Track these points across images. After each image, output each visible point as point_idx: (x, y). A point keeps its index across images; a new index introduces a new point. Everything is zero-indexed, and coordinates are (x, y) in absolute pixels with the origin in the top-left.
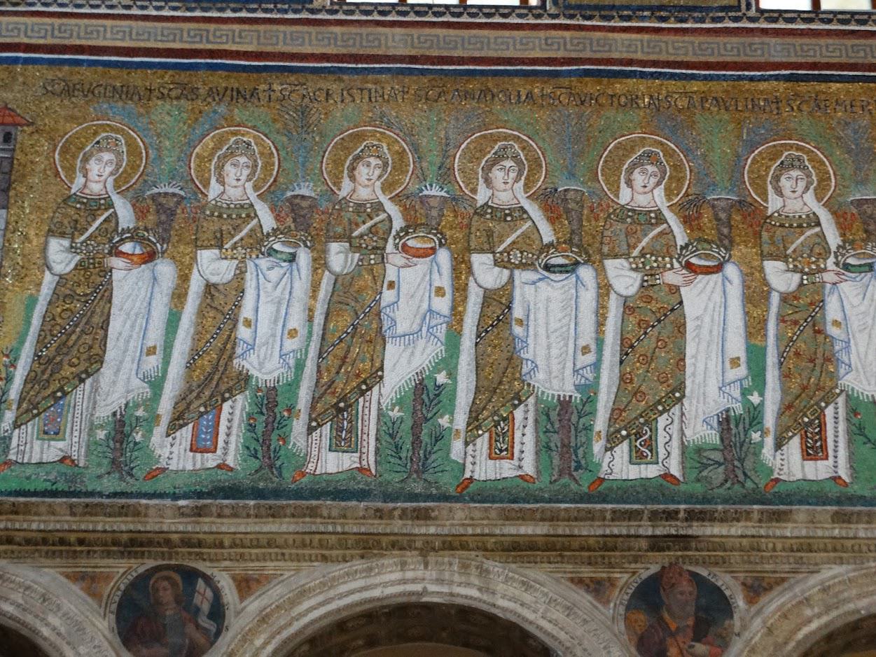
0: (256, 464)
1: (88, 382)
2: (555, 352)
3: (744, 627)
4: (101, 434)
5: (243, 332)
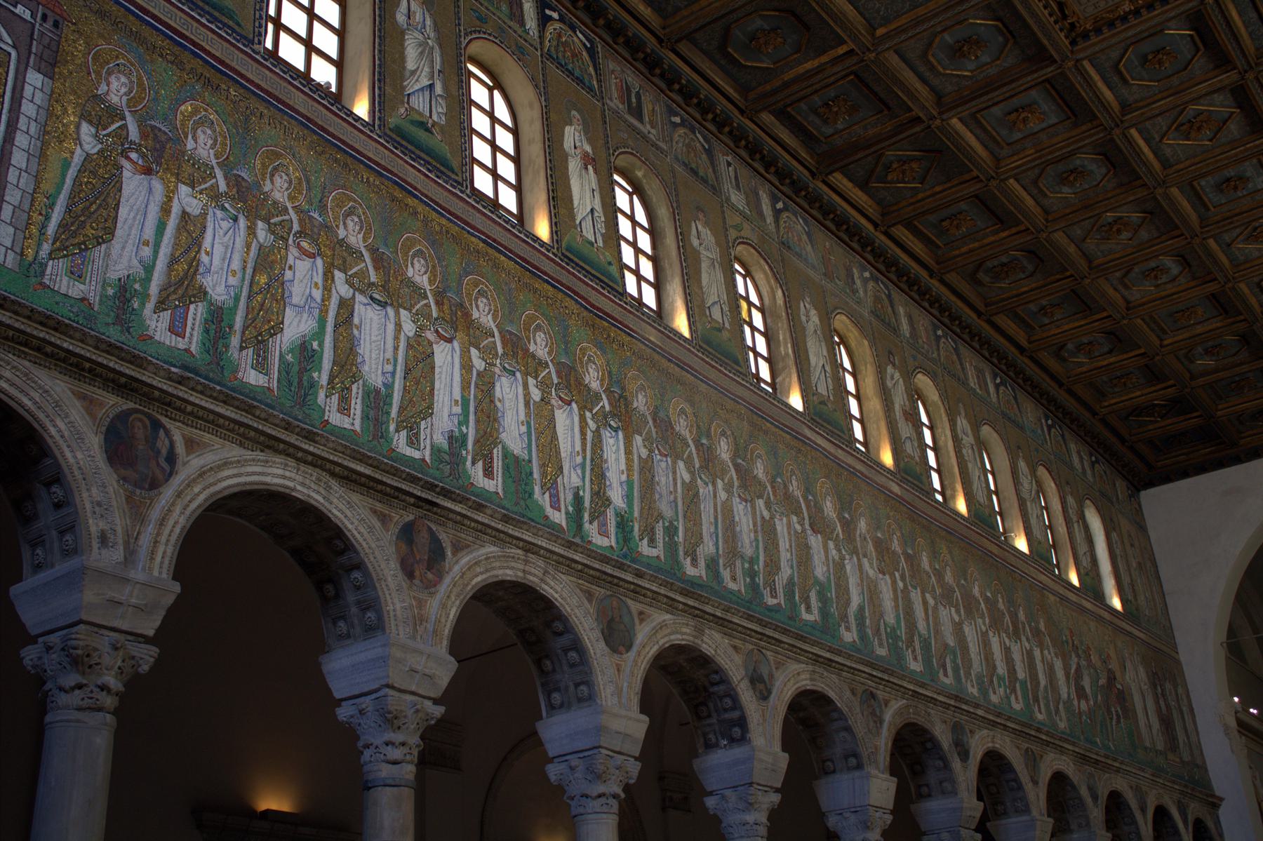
0: (208, 358)
1: (104, 246)
2: (374, 356)
3: (450, 569)
4: (110, 292)
5: (204, 258)
